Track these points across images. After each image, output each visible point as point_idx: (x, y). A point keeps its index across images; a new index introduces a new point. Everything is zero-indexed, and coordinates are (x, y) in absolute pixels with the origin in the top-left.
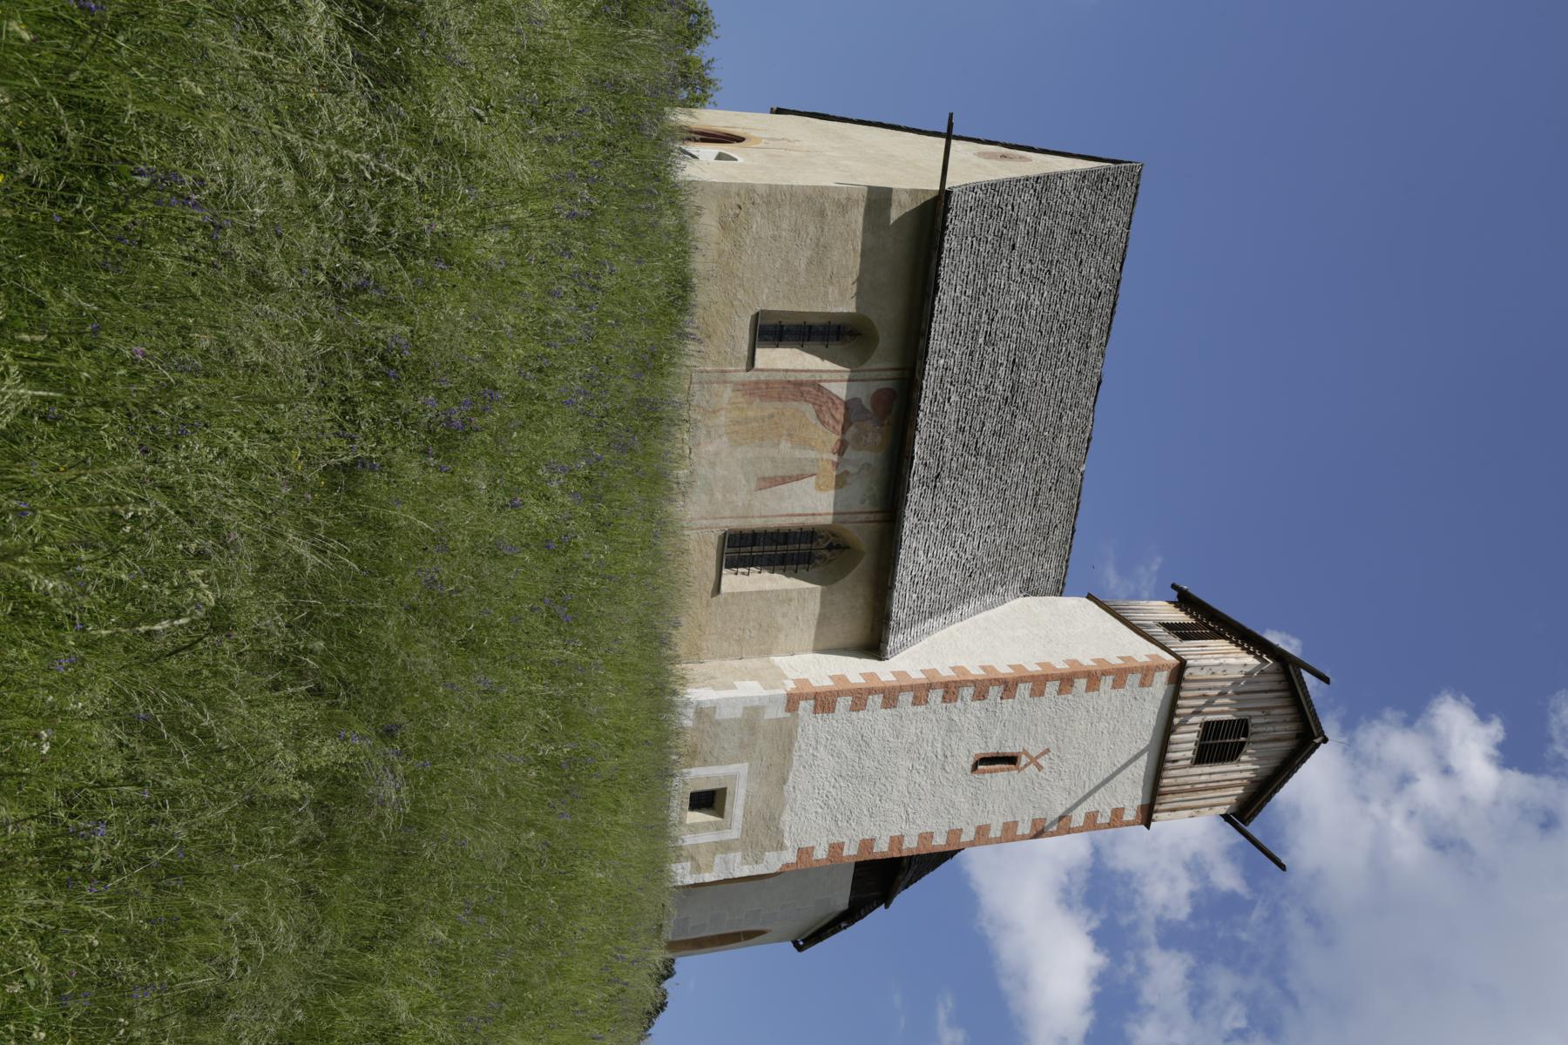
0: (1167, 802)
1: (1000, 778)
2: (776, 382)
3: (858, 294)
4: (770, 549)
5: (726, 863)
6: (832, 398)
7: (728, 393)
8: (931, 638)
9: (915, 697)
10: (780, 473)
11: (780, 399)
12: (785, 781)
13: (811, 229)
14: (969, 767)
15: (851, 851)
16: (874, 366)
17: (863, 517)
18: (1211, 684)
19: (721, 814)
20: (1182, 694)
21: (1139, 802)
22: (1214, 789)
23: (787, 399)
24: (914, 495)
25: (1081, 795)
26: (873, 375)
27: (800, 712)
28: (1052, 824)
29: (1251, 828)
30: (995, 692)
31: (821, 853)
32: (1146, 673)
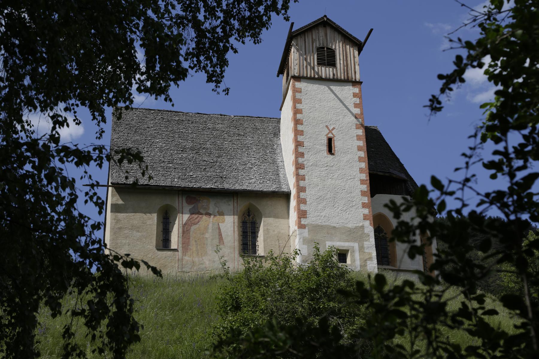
1: (337, 144)
3: (150, 213)
4: (250, 238)
5: (368, 247)
6: (189, 220)
7: (186, 258)
8: (287, 174)
9: (302, 180)
10: (217, 236)
11: (189, 239)
12: (334, 227)
13: (126, 232)
14: (332, 157)
15: (366, 200)
16: (177, 205)
17: (235, 204)
19: (347, 251)
20: (305, 75)
21: (351, 87)
22: (347, 57)
23: (189, 236)
24: (226, 186)
25: (347, 111)
26: (180, 205)
27: (306, 223)
28: (359, 121)
29: (362, 40)
30: (301, 150)
31: (366, 211)
32: (296, 91)
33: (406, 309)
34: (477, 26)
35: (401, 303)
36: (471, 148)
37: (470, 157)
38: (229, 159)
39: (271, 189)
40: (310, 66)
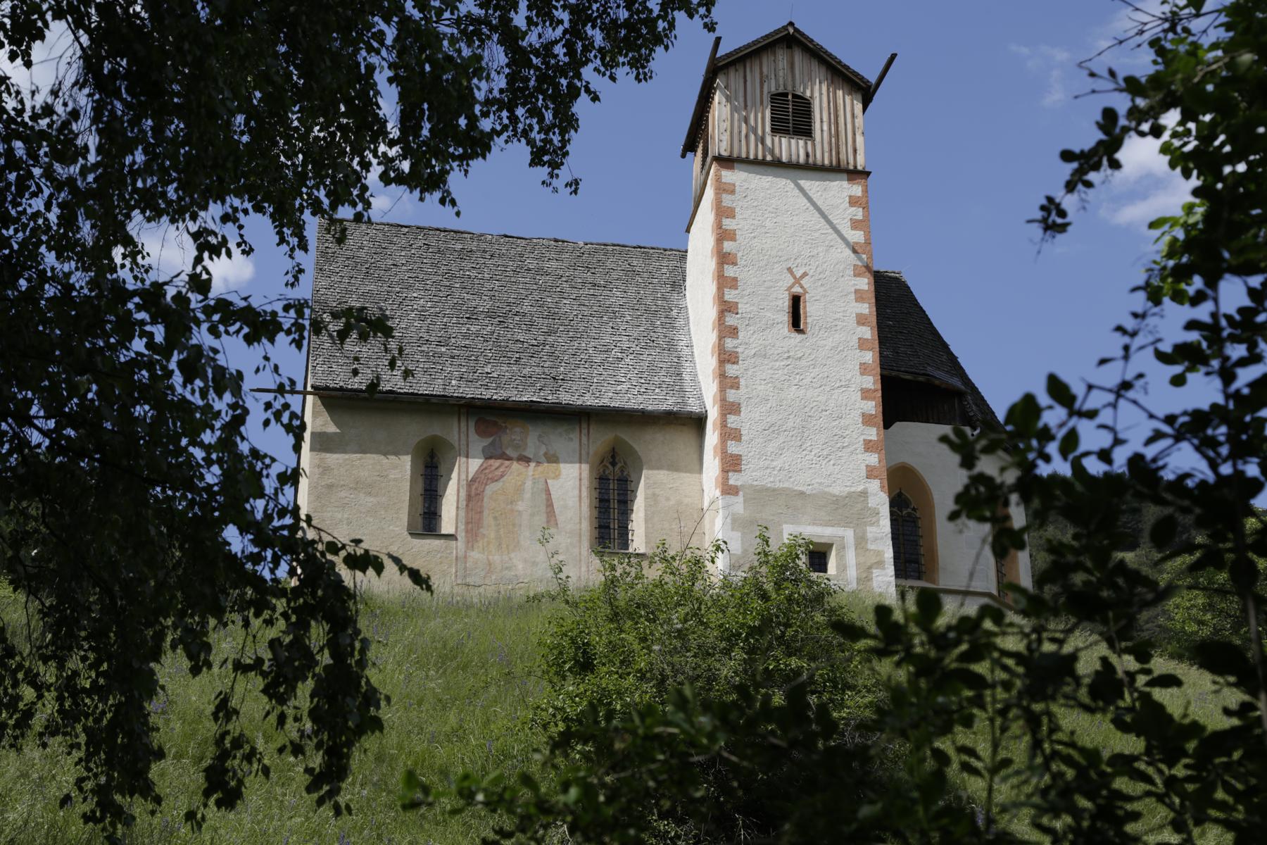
0: (847, 158)
1: (811, 310)
2: (467, 516)
3: (396, 454)
4: (615, 514)
5: (876, 539)
6: (481, 470)
7: (475, 555)
8: (699, 373)
9: (732, 387)
10: (543, 508)
11: (481, 512)
12: (802, 493)
13: (343, 494)
14: (799, 337)
15: (873, 433)
17: (584, 439)
18: (736, 131)
20: (744, 155)
21: (845, 184)
22: (837, 117)
23: (481, 507)
24: (565, 398)
25: (835, 236)
26: (463, 437)
27: (739, 483)
28: (860, 259)
29: (873, 79)
30: (731, 320)
31: (873, 459)
32: (722, 189)
33: (981, 668)
34: (1146, 46)
35: (975, 654)
36: (1135, 315)
37: (1134, 334)
38: (572, 339)
39: (663, 407)
40: (756, 134)
